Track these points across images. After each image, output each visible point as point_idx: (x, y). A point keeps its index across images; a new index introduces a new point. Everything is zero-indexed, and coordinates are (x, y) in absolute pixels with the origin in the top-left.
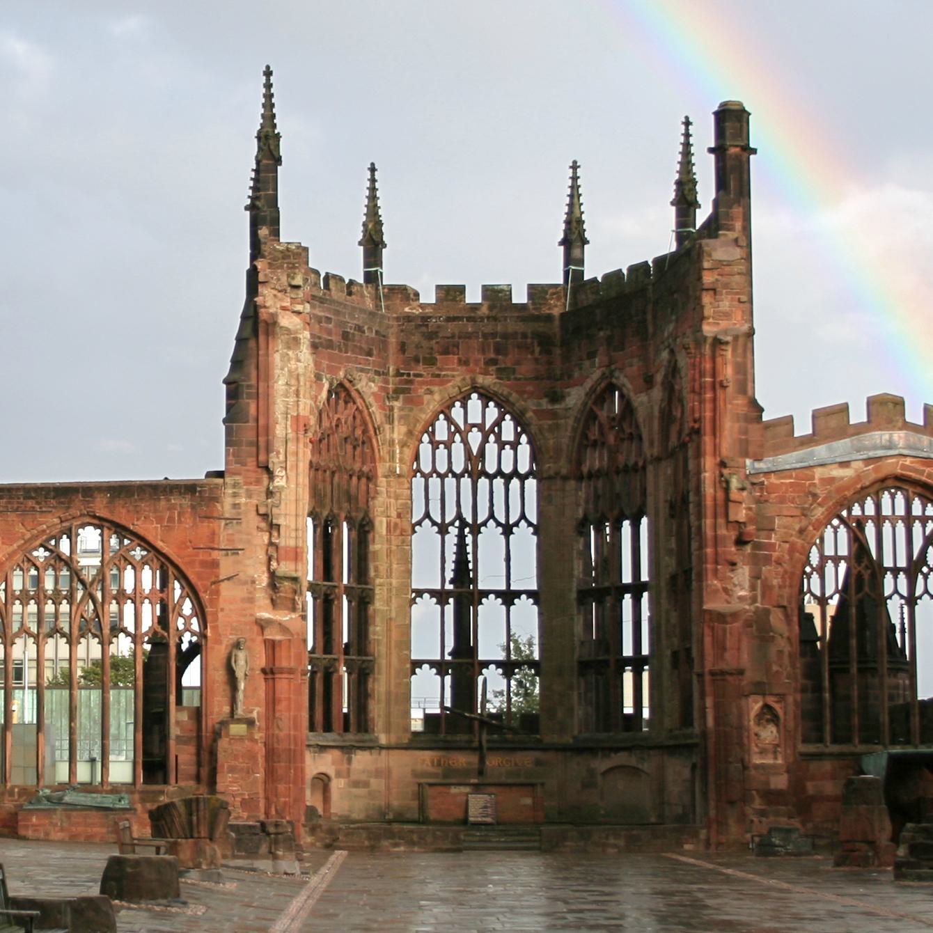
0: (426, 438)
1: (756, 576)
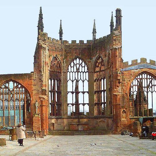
0: (70, 66)
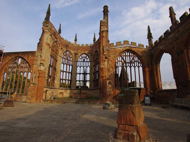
1: (108, 63)
